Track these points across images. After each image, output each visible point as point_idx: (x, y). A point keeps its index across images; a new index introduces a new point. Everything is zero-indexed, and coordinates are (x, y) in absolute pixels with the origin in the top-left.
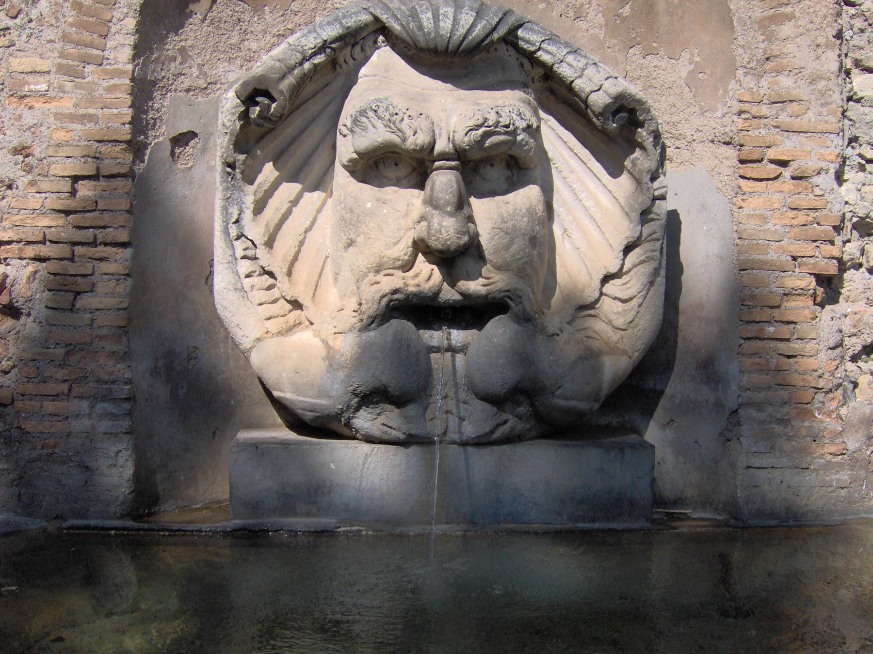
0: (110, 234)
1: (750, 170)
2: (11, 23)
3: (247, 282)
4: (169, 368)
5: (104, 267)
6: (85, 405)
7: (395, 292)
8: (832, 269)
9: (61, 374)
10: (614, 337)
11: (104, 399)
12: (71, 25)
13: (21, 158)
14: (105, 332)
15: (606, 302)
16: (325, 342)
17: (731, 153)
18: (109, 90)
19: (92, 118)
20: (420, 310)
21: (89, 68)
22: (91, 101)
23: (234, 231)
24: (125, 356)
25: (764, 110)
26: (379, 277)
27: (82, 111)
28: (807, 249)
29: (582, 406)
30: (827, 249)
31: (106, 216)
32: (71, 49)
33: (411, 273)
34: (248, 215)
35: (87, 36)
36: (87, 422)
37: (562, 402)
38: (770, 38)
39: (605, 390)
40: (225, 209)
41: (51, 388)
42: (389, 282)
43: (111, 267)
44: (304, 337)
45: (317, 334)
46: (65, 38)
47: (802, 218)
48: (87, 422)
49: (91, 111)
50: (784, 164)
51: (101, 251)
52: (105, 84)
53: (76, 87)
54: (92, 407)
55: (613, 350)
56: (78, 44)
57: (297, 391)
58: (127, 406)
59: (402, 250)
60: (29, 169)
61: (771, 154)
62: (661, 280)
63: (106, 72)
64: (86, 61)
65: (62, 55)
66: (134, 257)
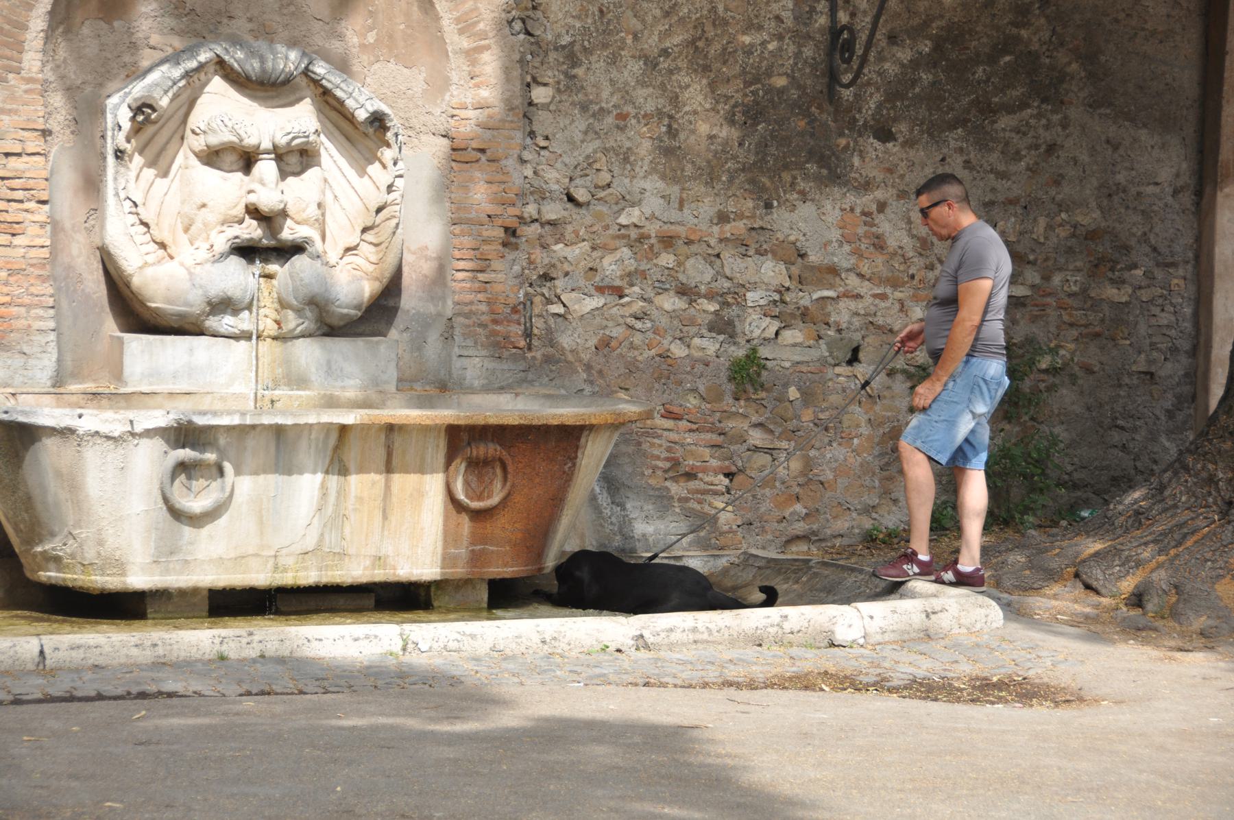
3: (133, 230)
5: (29, 216)
6: (23, 310)
7: (237, 237)
11: (37, 306)
14: (34, 261)
18: (26, 92)
21: (11, 76)
23: (122, 195)
26: (224, 228)
27: (9, 107)
31: (31, 181)
38: (474, 63)
40: (115, 179)
43: (37, 218)
45: (182, 264)
50: (483, 151)
52: (24, 87)
58: (52, 312)
59: (240, 210)
63: (23, 79)
64: (10, 70)
66: (51, 209)
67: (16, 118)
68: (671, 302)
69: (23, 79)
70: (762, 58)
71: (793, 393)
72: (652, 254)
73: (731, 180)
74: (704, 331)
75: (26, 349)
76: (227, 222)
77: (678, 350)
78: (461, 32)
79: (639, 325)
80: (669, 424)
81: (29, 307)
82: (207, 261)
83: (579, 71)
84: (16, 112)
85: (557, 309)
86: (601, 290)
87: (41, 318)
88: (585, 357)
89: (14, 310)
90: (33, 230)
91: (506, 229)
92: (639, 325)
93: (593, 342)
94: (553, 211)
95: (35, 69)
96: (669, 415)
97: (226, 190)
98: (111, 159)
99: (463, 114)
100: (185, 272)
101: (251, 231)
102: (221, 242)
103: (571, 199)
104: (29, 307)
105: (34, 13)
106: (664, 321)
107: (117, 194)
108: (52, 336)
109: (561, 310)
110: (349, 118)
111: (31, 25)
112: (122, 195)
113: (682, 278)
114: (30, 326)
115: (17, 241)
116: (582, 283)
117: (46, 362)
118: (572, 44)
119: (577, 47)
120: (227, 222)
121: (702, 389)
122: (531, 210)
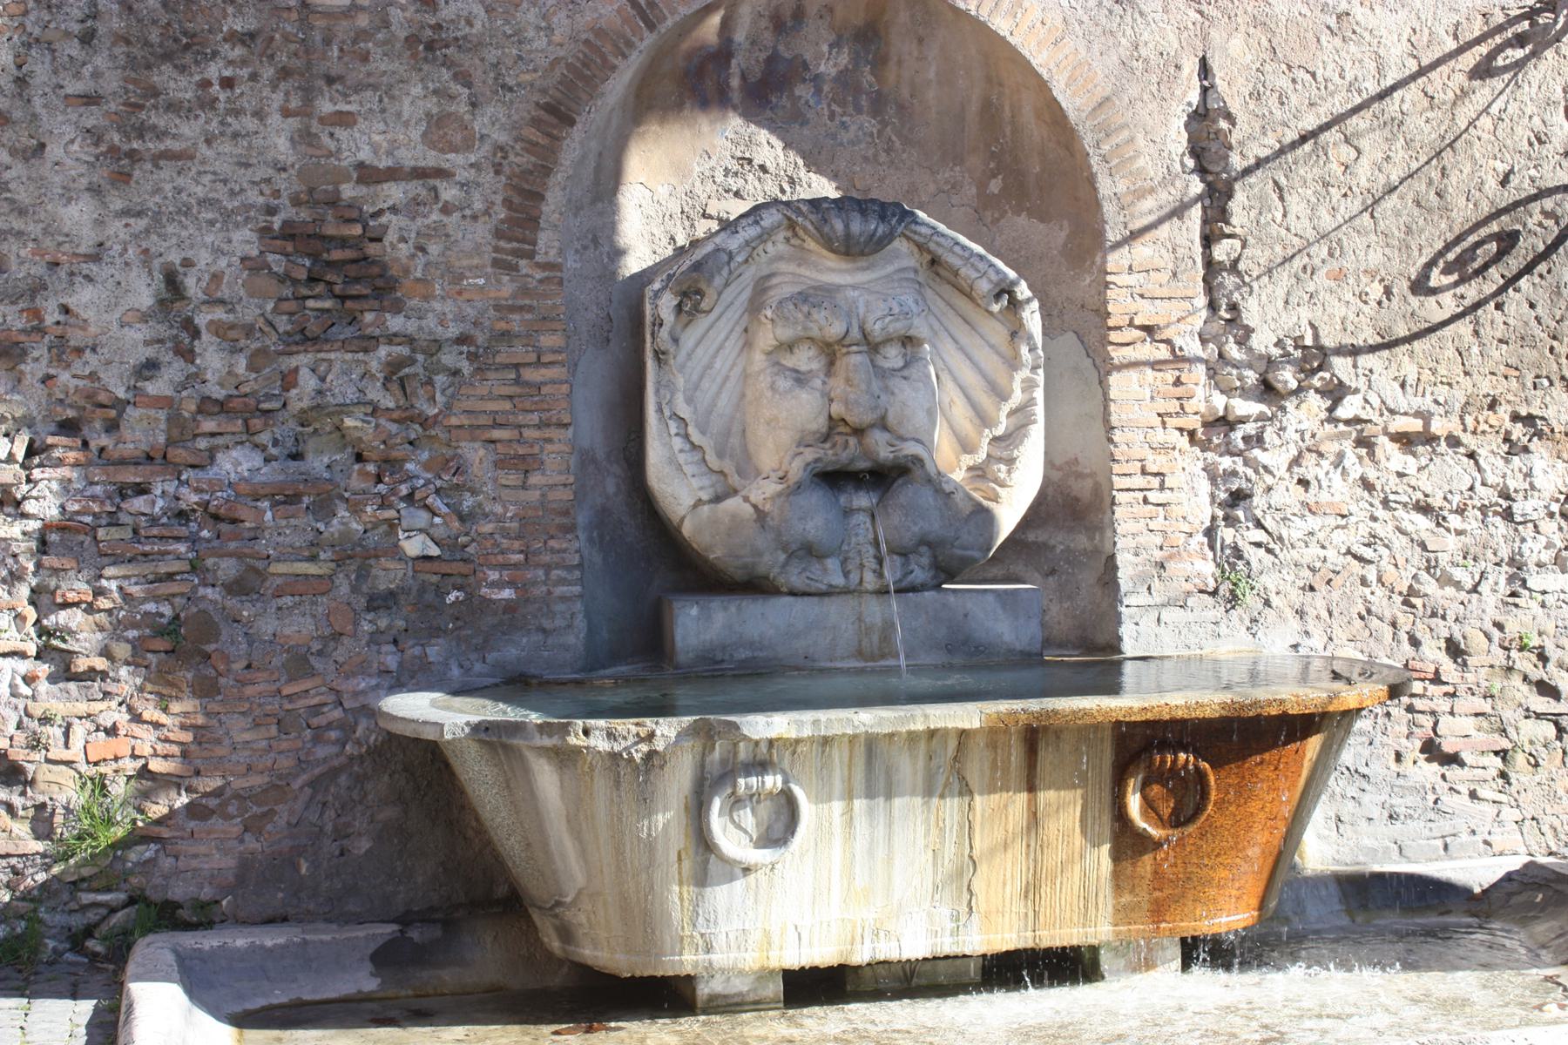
2: (445, 219)
9: (517, 545)
11: (558, 566)
12: (502, 221)
13: (465, 348)
14: (555, 506)
16: (755, 507)
18: (541, 281)
19: (530, 309)
21: (523, 263)
23: (667, 413)
27: (521, 302)
32: (502, 244)
33: (827, 445)
34: (680, 399)
35: (518, 232)
36: (544, 589)
37: (959, 552)
42: (810, 455)
44: (732, 504)
45: (746, 499)
46: (498, 234)
48: (544, 589)
49: (527, 302)
51: (548, 433)
52: (538, 276)
53: (512, 281)
54: (547, 574)
56: (510, 240)
58: (577, 573)
59: (821, 424)
60: (472, 357)
63: (538, 265)
64: (518, 253)
65: (497, 249)
67: (528, 316)
69: (538, 265)
75: (547, 624)
81: (548, 568)
82: (779, 495)
84: (530, 309)
87: (562, 581)
95: (553, 252)
100: (751, 510)
102: (796, 470)
104: (548, 568)
105: (552, 181)
107: (660, 410)
108: (579, 606)
111: (548, 195)
112: (667, 413)
114: (549, 593)
115: (535, 479)
117: (571, 639)
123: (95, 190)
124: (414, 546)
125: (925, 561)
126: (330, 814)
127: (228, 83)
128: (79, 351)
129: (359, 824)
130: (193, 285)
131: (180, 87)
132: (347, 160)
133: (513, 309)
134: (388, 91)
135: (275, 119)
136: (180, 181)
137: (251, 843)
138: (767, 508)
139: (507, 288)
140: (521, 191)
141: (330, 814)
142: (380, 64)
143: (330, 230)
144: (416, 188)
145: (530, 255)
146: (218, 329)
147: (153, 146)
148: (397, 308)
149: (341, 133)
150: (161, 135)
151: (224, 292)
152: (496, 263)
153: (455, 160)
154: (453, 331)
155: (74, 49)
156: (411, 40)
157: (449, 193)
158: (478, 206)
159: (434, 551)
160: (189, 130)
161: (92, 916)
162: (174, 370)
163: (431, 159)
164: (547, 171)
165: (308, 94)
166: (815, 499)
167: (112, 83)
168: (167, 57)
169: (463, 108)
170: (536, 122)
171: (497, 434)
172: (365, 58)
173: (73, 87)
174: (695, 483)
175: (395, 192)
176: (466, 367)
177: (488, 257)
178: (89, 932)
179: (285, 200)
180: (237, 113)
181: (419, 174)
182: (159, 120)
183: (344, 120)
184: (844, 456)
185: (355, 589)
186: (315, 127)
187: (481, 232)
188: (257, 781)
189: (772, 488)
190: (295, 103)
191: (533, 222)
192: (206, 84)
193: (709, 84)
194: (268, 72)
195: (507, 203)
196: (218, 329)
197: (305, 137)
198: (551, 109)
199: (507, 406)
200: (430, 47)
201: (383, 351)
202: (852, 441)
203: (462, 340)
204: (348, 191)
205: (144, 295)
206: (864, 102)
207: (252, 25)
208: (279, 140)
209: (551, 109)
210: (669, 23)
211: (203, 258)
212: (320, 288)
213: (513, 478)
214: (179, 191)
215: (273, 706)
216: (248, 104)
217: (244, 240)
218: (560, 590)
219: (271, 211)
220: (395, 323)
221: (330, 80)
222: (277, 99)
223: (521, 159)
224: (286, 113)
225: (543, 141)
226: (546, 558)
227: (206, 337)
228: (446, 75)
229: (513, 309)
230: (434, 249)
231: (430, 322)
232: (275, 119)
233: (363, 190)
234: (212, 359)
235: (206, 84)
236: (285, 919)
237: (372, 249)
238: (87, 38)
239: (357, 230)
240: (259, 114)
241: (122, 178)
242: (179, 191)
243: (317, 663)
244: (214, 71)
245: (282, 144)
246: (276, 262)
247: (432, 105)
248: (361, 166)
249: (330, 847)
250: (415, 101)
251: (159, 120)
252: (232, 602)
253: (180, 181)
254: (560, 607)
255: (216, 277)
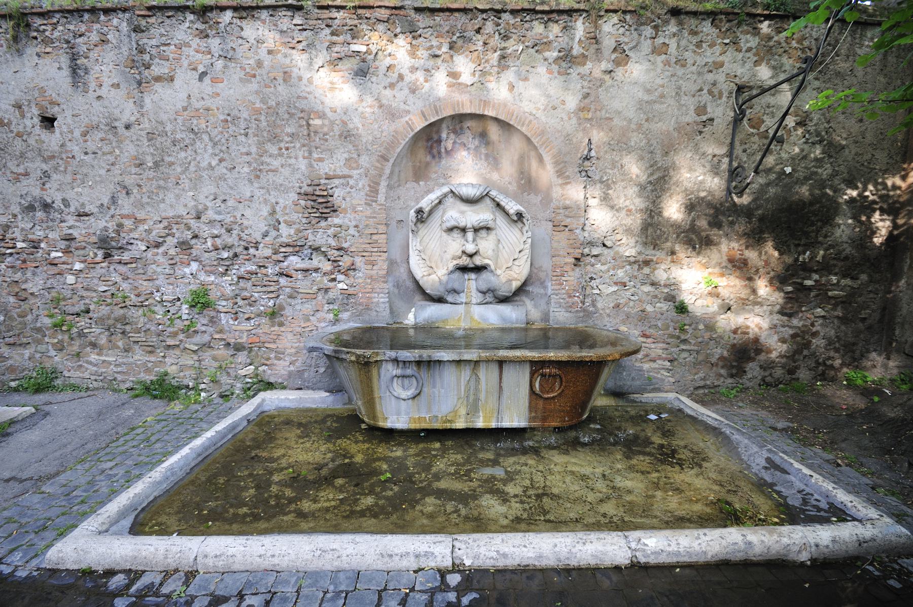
0: (381, 249)
1: (555, 229)
4: (398, 285)
8: (579, 256)
10: (516, 276)
15: (514, 267)
17: (551, 223)
19: (375, 217)
20: (464, 269)
22: (374, 212)
24: (386, 282)
25: (561, 211)
28: (572, 251)
29: (507, 294)
30: (578, 251)
39: (513, 290)
41: (367, 290)
42: (455, 262)
44: (433, 277)
47: (571, 242)
55: (516, 279)
57: (432, 290)
59: (459, 253)
60: (358, 232)
61: (563, 224)
62: (529, 260)
68: (647, 288)
70: (695, 184)
71: (701, 327)
72: (640, 268)
73: (678, 237)
74: (662, 300)
76: (454, 258)
77: (649, 308)
78: (558, 176)
79: (632, 298)
80: (644, 340)
83: (610, 192)
84: (375, 217)
85: (597, 291)
86: (616, 284)
88: (608, 311)
89: (373, 295)
90: (380, 263)
91: (576, 259)
92: (632, 298)
93: (612, 305)
94: (595, 251)
96: (645, 336)
97: (456, 245)
98: (411, 234)
99: (558, 211)
101: (465, 261)
102: (451, 265)
103: (604, 245)
104: (379, 294)
106: (644, 297)
108: (387, 305)
109: (598, 292)
110: (507, 213)
113: (653, 278)
115: (375, 268)
116: (608, 281)
118: (608, 180)
119: (610, 182)
120: (454, 258)
121: (660, 325)
122: (586, 251)
123: (250, 181)
124: (342, 286)
125: (491, 295)
126: (314, 360)
127: (287, 149)
128: (247, 228)
129: (322, 364)
130: (278, 209)
131: (273, 150)
132: (322, 172)
133: (370, 217)
134: (331, 152)
135: (301, 159)
136: (274, 178)
137: (292, 368)
138: (442, 278)
139: (368, 212)
140: (374, 183)
141: (314, 360)
142: (332, 143)
143: (318, 193)
144: (342, 181)
145: (376, 202)
146: (285, 222)
147: (264, 167)
148: (337, 216)
149: (320, 164)
150: (268, 164)
151: (287, 211)
152: (366, 204)
153: (355, 173)
154: (354, 223)
155: (243, 138)
156: (340, 136)
157: (351, 182)
158: (360, 185)
159: (346, 287)
160: (276, 163)
161: (249, 385)
162: (273, 233)
163: (346, 172)
164: (381, 176)
165: (310, 153)
166: (458, 274)
167: (254, 150)
168: (269, 141)
169: (355, 156)
170: (378, 161)
171: (364, 254)
172: (326, 140)
173: (244, 150)
174: (423, 270)
175: (337, 182)
176: (357, 234)
177: (362, 203)
178: (249, 389)
179: (305, 184)
180: (290, 158)
181: (344, 177)
182: (268, 160)
183: (321, 160)
184: (466, 263)
185: (323, 298)
186: (313, 162)
187: (362, 193)
188: (293, 351)
189: (444, 271)
190: (306, 154)
191: (377, 192)
192: (280, 149)
193: (435, 151)
194: (298, 145)
195: (369, 186)
196: (285, 222)
197: (311, 166)
198: (382, 157)
199: (368, 246)
200: (346, 138)
201: (333, 229)
202: (468, 259)
203: (356, 226)
204: (323, 181)
205: (265, 211)
206: (483, 157)
207: (294, 131)
208: (302, 165)
209: (382, 157)
210: (418, 129)
211: (281, 201)
212: (315, 210)
213: (370, 267)
214: (274, 181)
215: (299, 329)
216: (293, 155)
217: (293, 196)
218: (382, 300)
219: (301, 188)
220: (336, 221)
221: (317, 148)
222: (302, 153)
223: (373, 172)
224: (304, 158)
225: (379, 166)
226: (378, 290)
227: (282, 224)
228: (351, 146)
229: (370, 217)
230: (348, 199)
231: (346, 221)
232: (301, 159)
233: (327, 181)
234: (284, 230)
235: (280, 149)
236: (301, 389)
237: (330, 199)
238: (246, 135)
239: (325, 193)
240: (296, 158)
241: (258, 177)
242: (274, 181)
243: (311, 318)
244: (282, 145)
245: (303, 167)
246: (303, 203)
247: (346, 155)
248: (326, 174)
249: (313, 369)
250: (341, 156)
251: (268, 160)
252: (289, 300)
253: (274, 178)
254: (382, 305)
255: (285, 207)
